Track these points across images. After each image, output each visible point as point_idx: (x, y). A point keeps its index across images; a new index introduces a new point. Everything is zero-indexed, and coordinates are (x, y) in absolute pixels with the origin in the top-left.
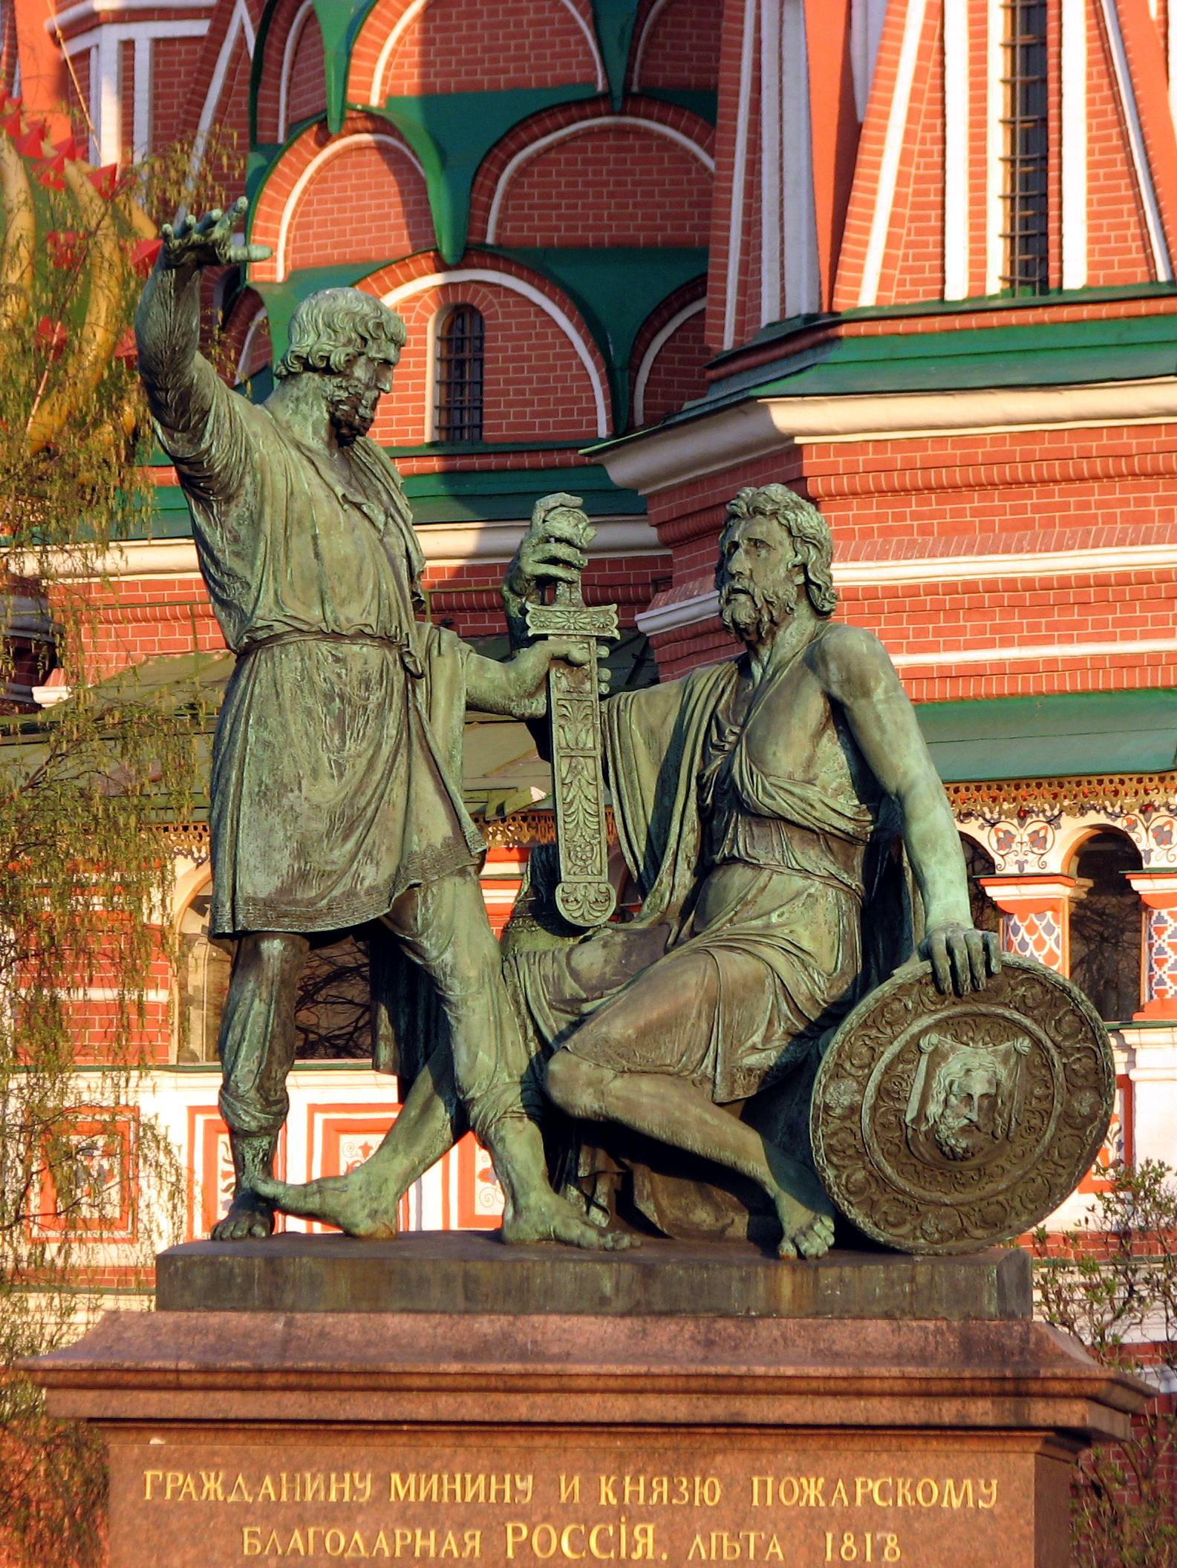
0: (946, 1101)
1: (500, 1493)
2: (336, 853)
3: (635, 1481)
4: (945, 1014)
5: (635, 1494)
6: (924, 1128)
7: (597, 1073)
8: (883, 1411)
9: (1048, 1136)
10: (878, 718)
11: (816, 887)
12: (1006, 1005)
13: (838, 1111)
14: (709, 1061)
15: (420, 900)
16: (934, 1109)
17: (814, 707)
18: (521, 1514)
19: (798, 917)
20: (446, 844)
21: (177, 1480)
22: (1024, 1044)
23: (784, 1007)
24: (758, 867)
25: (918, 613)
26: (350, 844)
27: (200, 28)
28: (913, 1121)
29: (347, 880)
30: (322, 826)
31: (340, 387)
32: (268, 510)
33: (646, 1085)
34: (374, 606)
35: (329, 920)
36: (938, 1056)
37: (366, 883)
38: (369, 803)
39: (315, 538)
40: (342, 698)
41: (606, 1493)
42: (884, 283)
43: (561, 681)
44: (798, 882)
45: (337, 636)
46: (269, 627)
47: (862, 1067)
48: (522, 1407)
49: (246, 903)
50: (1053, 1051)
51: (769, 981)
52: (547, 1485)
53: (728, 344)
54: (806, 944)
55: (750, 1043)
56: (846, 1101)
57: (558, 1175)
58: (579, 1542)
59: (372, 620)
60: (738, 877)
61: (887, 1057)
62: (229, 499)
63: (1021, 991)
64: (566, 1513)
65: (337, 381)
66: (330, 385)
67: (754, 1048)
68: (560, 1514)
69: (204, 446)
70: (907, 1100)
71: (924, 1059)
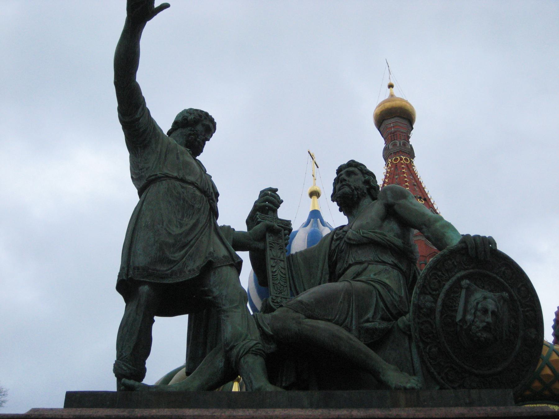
0: (475, 313)
2: (176, 255)
4: (471, 271)
6: (465, 327)
7: (297, 315)
9: (518, 347)
10: (411, 203)
11: (388, 267)
12: (497, 274)
13: (425, 310)
14: (348, 319)
15: (212, 273)
16: (469, 317)
19: (383, 275)
20: (224, 256)
22: (505, 294)
23: (381, 304)
24: (361, 263)
26: (183, 252)
28: (460, 321)
29: (180, 264)
30: (171, 241)
31: (191, 130)
32: (160, 146)
33: (320, 321)
34: (199, 180)
35: (170, 279)
36: (469, 292)
37: (189, 268)
38: (192, 240)
39: (178, 153)
40: (184, 200)
43: (270, 239)
44: (381, 267)
45: (183, 180)
46: (156, 175)
47: (435, 290)
49: (134, 268)
50: (518, 303)
51: (374, 292)
54: (387, 281)
55: (366, 318)
56: (428, 304)
59: (199, 183)
61: (447, 286)
62: (145, 147)
63: (503, 269)
65: (189, 128)
66: (187, 131)
67: (368, 321)
69: (137, 116)
70: (456, 311)
71: (463, 293)
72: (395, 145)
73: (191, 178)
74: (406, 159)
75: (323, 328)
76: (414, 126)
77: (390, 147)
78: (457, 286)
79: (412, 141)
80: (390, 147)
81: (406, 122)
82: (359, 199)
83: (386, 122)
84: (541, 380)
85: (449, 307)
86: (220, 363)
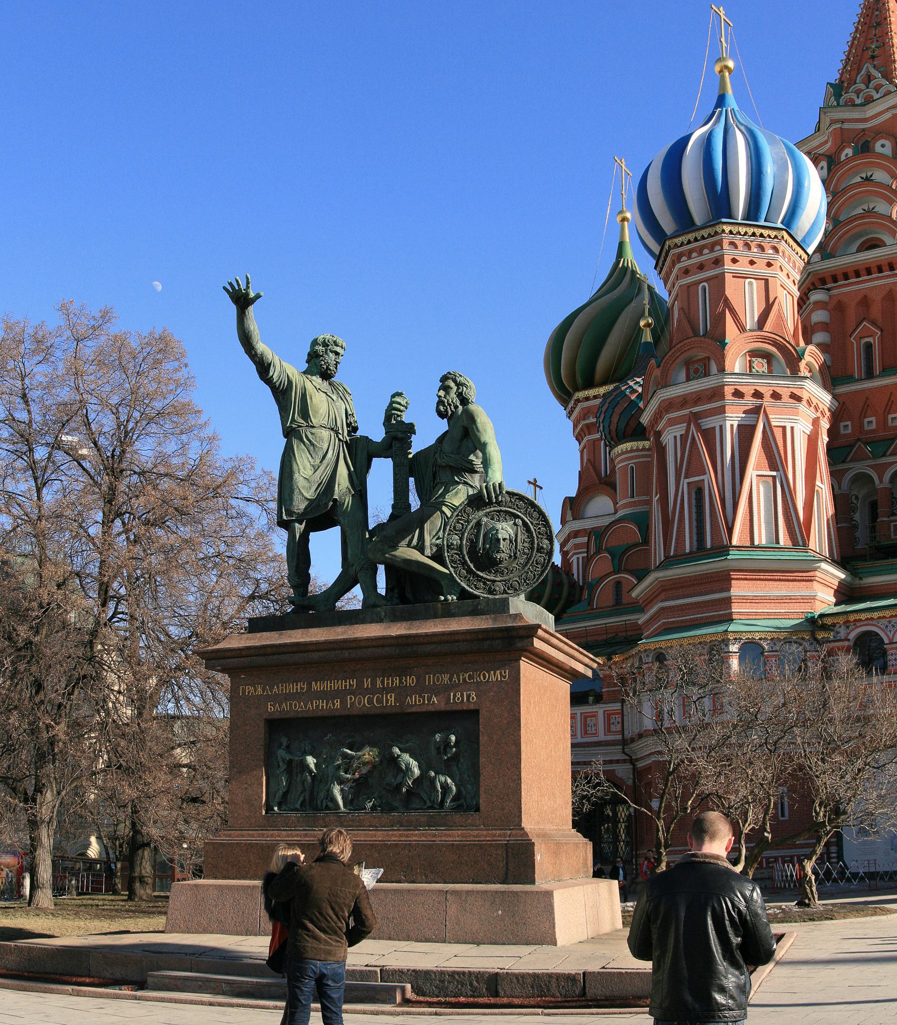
1: (346, 686)
3: (388, 679)
5: (388, 683)
18: (352, 692)
25: (682, 610)
42: (675, 551)
52: (360, 684)
58: (370, 701)
64: (367, 691)
68: (365, 692)
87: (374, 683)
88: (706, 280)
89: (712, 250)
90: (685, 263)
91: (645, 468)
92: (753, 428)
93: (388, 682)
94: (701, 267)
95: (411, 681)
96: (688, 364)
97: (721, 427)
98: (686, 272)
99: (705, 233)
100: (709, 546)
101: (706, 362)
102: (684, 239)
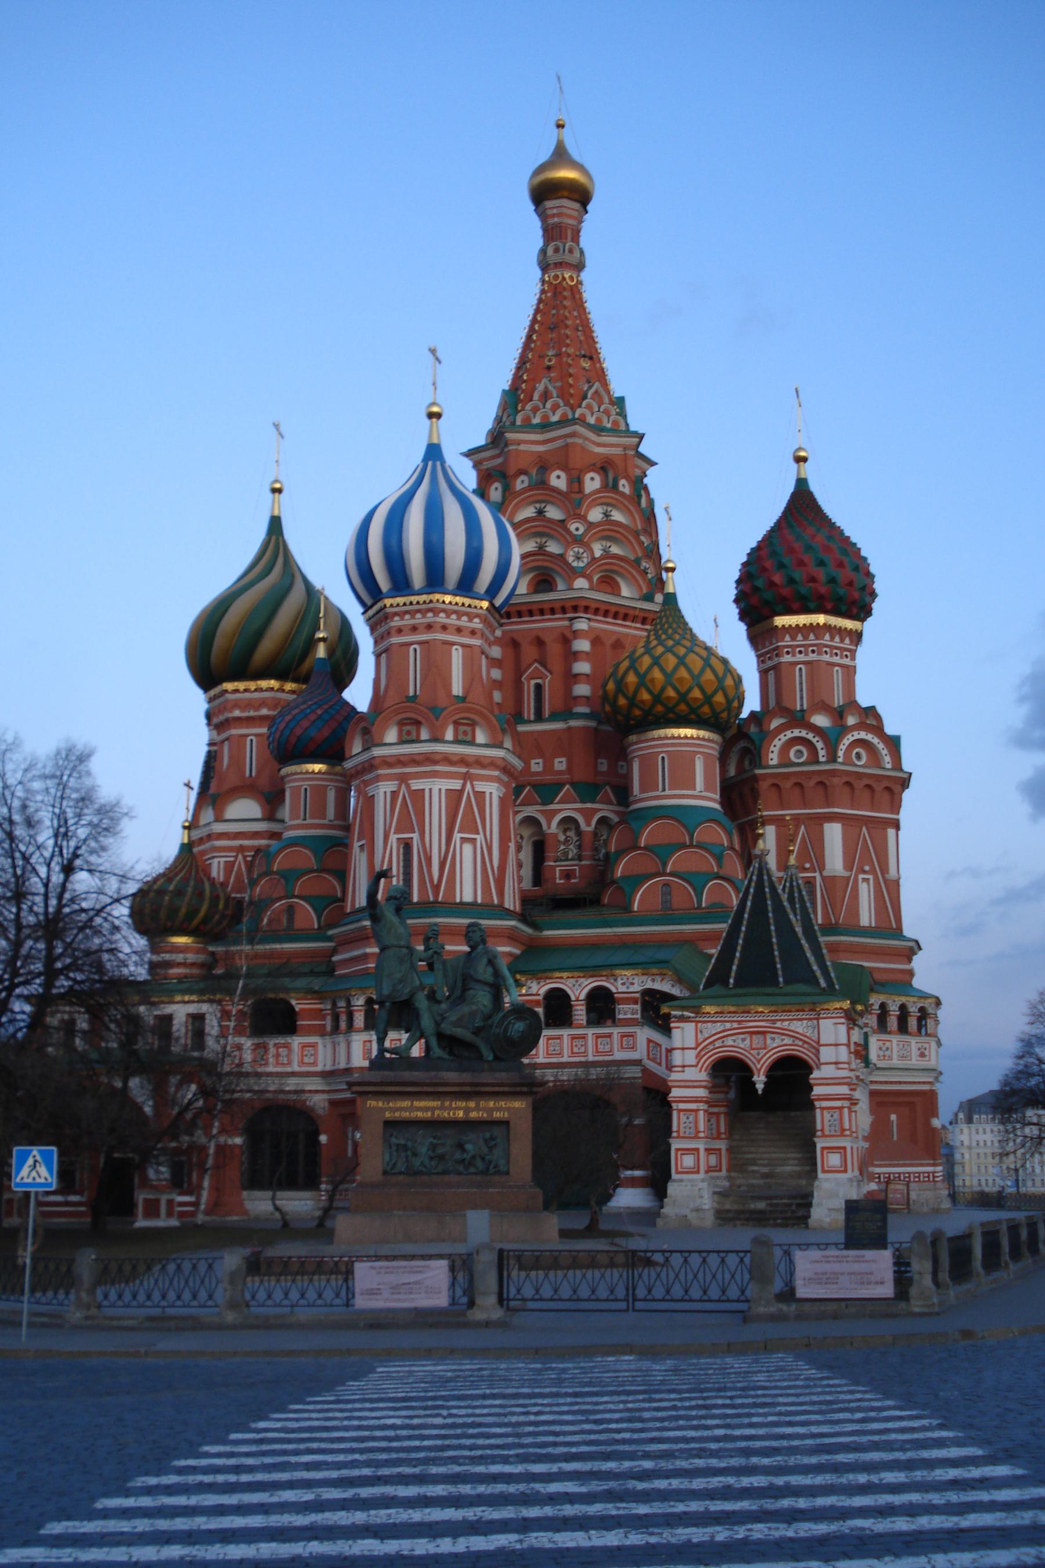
8: (506, 1089)
17: (485, 961)
18: (437, 1108)
19: (483, 998)
21: (373, 1103)
27: (232, 859)
41: (454, 1105)
43: (436, 956)
48: (441, 1089)
53: (348, 911)
57: (440, 1046)
60: (472, 992)
64: (445, 1109)
66: (397, 902)
72: (556, 250)
73: (403, 943)
74: (571, 278)
75: (459, 1032)
76: (589, 208)
77: (550, 251)
78: (510, 1023)
79: (586, 240)
80: (550, 251)
81: (577, 206)
82: (478, 945)
83: (549, 204)
84: (688, 704)
85: (506, 1030)
86: (418, 1034)
87: (451, 1104)
88: (420, 643)
89: (424, 616)
90: (396, 622)
91: (320, 793)
92: (461, 792)
93: (459, 1104)
94: (414, 629)
95: (472, 1104)
96: (401, 724)
97: (430, 789)
98: (400, 631)
99: (422, 598)
100: (415, 899)
101: (418, 723)
102: (400, 600)
